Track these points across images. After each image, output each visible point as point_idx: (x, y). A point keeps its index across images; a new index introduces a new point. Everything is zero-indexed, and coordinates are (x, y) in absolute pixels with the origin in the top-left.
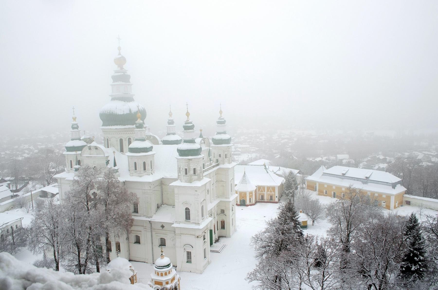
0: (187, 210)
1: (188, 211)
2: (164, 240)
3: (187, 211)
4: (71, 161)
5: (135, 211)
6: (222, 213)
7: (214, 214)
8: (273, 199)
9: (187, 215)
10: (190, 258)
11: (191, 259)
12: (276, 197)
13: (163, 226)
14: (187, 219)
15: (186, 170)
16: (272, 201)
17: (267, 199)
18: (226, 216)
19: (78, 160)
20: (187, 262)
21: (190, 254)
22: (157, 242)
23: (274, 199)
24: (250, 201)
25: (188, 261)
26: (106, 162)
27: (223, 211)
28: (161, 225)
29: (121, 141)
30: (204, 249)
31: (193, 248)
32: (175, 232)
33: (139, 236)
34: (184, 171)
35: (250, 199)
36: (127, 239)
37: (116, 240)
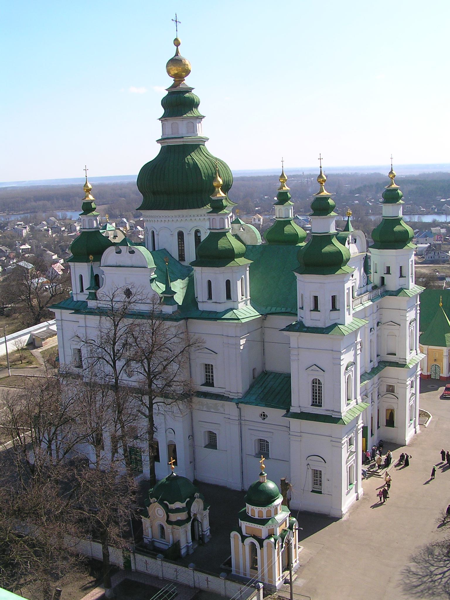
1: (317, 385)
2: (265, 443)
4: (81, 277)
5: (207, 382)
6: (388, 392)
7: (372, 394)
9: (315, 394)
10: (318, 484)
13: (264, 415)
14: (316, 402)
15: (316, 298)
18: (398, 398)
19: (95, 275)
20: (313, 491)
22: (251, 448)
25: (314, 489)
26: (150, 280)
27: (391, 388)
28: (261, 413)
29: (181, 235)
30: (349, 467)
31: (325, 463)
32: (289, 428)
33: (214, 433)
34: (312, 300)
36: (190, 437)
37: (169, 439)
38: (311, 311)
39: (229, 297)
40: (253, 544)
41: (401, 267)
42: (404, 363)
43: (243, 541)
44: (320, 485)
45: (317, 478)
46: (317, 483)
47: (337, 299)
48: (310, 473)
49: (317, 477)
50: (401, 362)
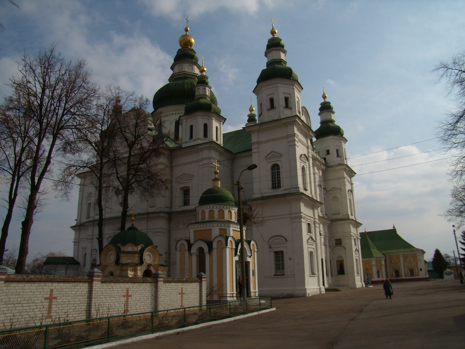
0: (275, 170)
3: (275, 172)
6: (337, 245)
8: (416, 273)
11: (283, 268)
12: (419, 270)
14: (276, 187)
15: (272, 100)
16: (413, 277)
17: (405, 274)
18: (345, 249)
21: (281, 255)
23: (417, 274)
24: (379, 276)
25: (277, 274)
27: (339, 242)
34: (269, 101)
35: (378, 272)
38: (268, 110)
39: (206, 135)
40: (201, 250)
41: (337, 150)
42: (347, 218)
43: (189, 249)
44: (283, 269)
45: (279, 263)
46: (279, 264)
47: (290, 99)
48: (272, 255)
49: (279, 258)
50: (345, 217)
